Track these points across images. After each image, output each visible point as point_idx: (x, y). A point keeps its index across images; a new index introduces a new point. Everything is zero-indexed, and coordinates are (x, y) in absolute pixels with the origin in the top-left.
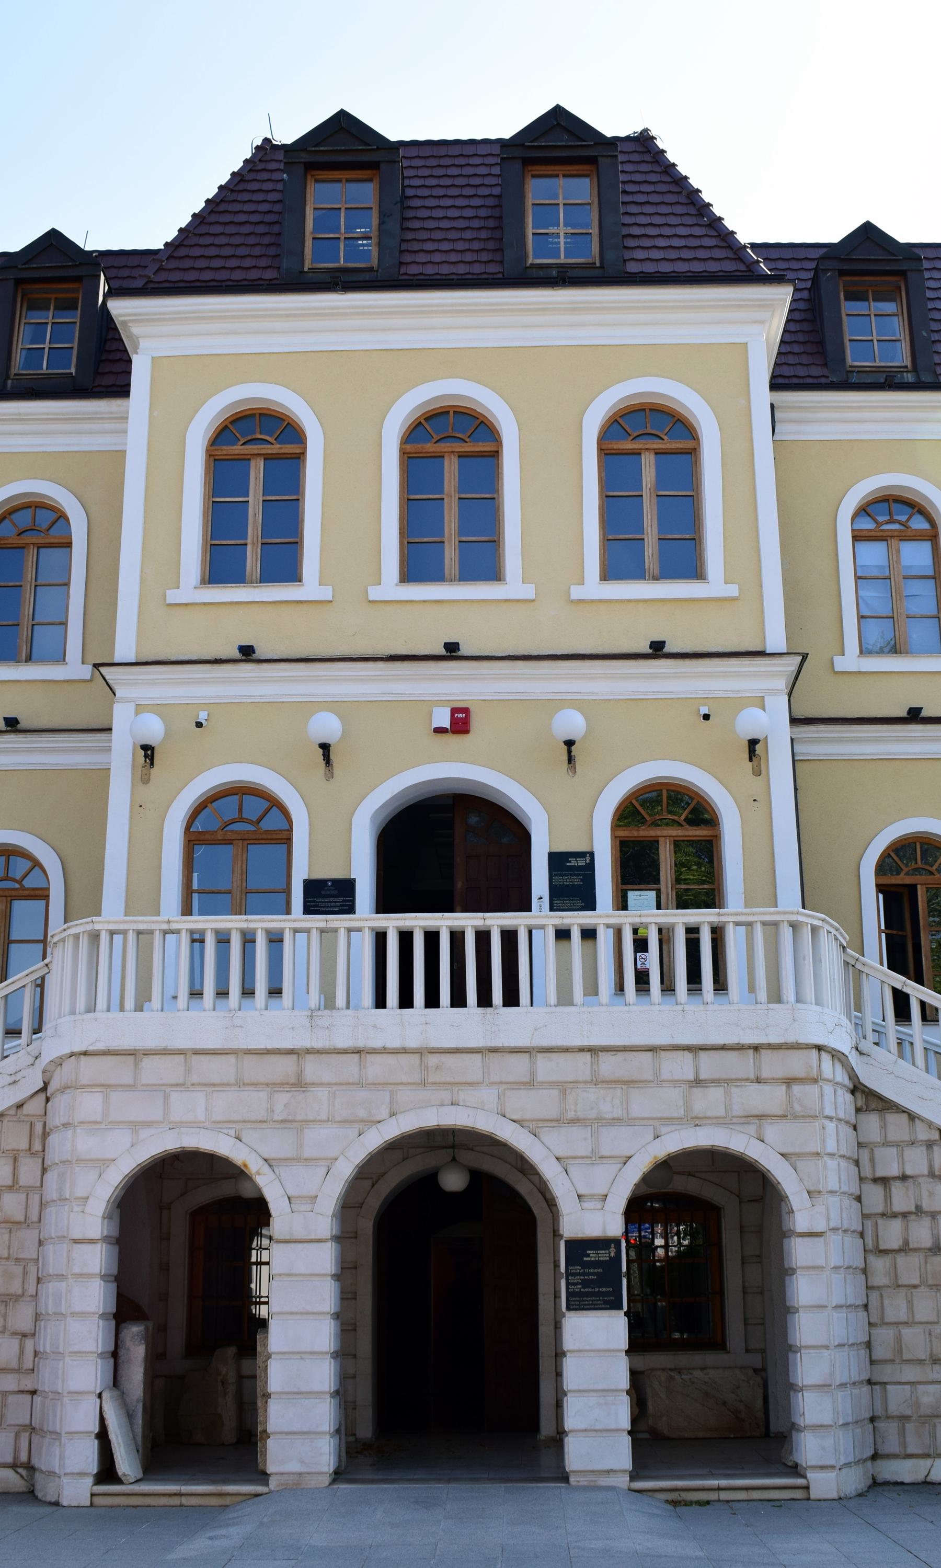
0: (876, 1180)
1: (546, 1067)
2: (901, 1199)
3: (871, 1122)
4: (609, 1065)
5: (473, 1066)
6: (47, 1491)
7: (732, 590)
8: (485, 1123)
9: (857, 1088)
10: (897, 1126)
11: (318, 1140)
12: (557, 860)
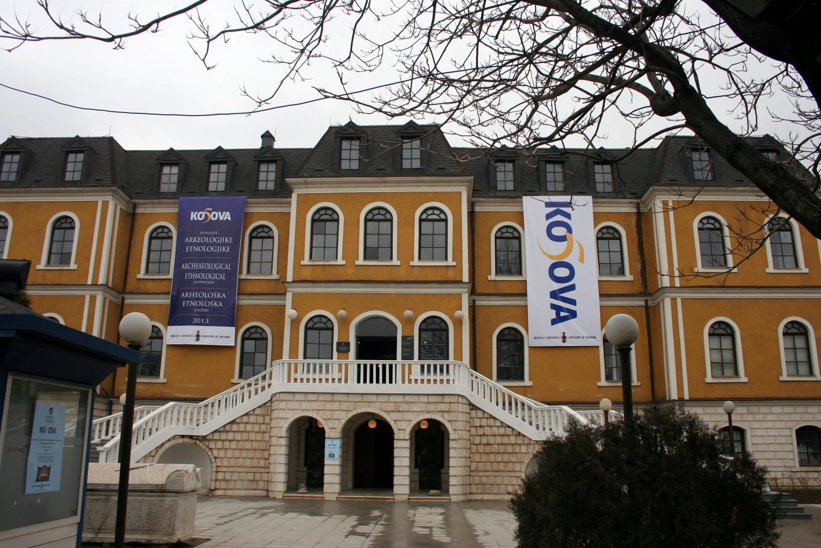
0: (474, 427)
1: (392, 399)
2: (480, 431)
3: (473, 413)
4: (407, 399)
5: (374, 398)
6: (271, 495)
7: (454, 264)
8: (376, 411)
9: (470, 404)
10: (480, 414)
11: (337, 415)
12: (404, 338)
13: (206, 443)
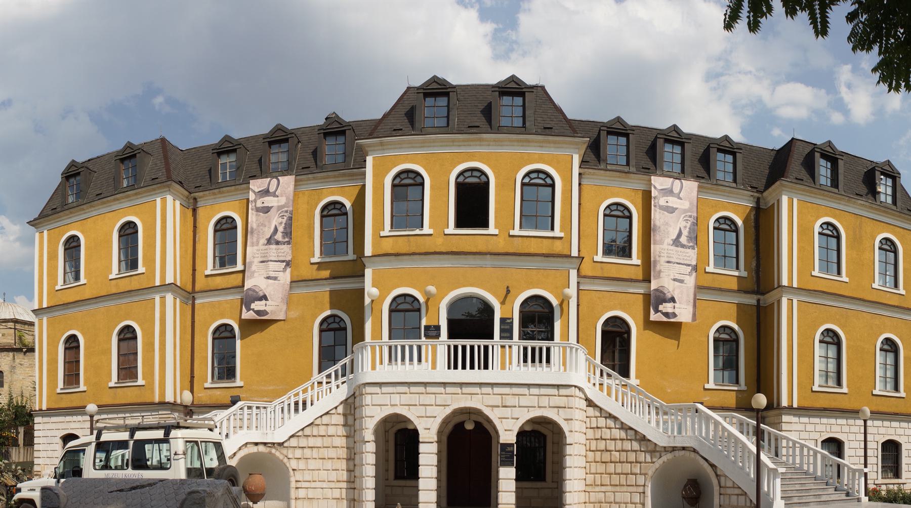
1: (497, 390)
8: (478, 406)
9: (587, 399)
12: (503, 320)
13: (285, 451)
